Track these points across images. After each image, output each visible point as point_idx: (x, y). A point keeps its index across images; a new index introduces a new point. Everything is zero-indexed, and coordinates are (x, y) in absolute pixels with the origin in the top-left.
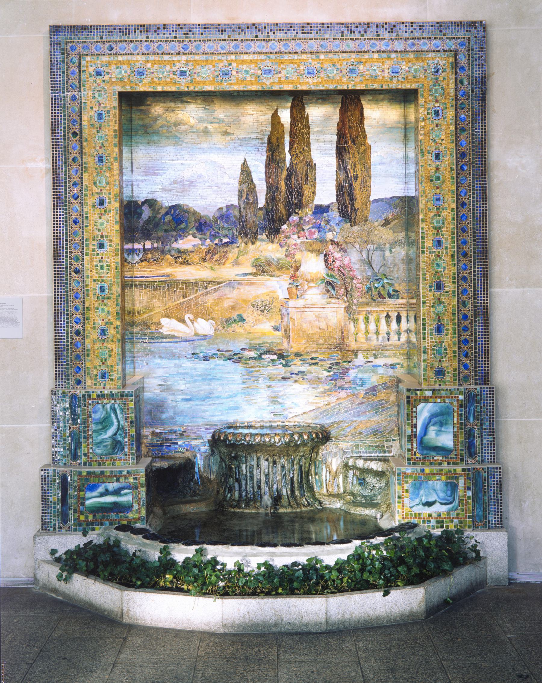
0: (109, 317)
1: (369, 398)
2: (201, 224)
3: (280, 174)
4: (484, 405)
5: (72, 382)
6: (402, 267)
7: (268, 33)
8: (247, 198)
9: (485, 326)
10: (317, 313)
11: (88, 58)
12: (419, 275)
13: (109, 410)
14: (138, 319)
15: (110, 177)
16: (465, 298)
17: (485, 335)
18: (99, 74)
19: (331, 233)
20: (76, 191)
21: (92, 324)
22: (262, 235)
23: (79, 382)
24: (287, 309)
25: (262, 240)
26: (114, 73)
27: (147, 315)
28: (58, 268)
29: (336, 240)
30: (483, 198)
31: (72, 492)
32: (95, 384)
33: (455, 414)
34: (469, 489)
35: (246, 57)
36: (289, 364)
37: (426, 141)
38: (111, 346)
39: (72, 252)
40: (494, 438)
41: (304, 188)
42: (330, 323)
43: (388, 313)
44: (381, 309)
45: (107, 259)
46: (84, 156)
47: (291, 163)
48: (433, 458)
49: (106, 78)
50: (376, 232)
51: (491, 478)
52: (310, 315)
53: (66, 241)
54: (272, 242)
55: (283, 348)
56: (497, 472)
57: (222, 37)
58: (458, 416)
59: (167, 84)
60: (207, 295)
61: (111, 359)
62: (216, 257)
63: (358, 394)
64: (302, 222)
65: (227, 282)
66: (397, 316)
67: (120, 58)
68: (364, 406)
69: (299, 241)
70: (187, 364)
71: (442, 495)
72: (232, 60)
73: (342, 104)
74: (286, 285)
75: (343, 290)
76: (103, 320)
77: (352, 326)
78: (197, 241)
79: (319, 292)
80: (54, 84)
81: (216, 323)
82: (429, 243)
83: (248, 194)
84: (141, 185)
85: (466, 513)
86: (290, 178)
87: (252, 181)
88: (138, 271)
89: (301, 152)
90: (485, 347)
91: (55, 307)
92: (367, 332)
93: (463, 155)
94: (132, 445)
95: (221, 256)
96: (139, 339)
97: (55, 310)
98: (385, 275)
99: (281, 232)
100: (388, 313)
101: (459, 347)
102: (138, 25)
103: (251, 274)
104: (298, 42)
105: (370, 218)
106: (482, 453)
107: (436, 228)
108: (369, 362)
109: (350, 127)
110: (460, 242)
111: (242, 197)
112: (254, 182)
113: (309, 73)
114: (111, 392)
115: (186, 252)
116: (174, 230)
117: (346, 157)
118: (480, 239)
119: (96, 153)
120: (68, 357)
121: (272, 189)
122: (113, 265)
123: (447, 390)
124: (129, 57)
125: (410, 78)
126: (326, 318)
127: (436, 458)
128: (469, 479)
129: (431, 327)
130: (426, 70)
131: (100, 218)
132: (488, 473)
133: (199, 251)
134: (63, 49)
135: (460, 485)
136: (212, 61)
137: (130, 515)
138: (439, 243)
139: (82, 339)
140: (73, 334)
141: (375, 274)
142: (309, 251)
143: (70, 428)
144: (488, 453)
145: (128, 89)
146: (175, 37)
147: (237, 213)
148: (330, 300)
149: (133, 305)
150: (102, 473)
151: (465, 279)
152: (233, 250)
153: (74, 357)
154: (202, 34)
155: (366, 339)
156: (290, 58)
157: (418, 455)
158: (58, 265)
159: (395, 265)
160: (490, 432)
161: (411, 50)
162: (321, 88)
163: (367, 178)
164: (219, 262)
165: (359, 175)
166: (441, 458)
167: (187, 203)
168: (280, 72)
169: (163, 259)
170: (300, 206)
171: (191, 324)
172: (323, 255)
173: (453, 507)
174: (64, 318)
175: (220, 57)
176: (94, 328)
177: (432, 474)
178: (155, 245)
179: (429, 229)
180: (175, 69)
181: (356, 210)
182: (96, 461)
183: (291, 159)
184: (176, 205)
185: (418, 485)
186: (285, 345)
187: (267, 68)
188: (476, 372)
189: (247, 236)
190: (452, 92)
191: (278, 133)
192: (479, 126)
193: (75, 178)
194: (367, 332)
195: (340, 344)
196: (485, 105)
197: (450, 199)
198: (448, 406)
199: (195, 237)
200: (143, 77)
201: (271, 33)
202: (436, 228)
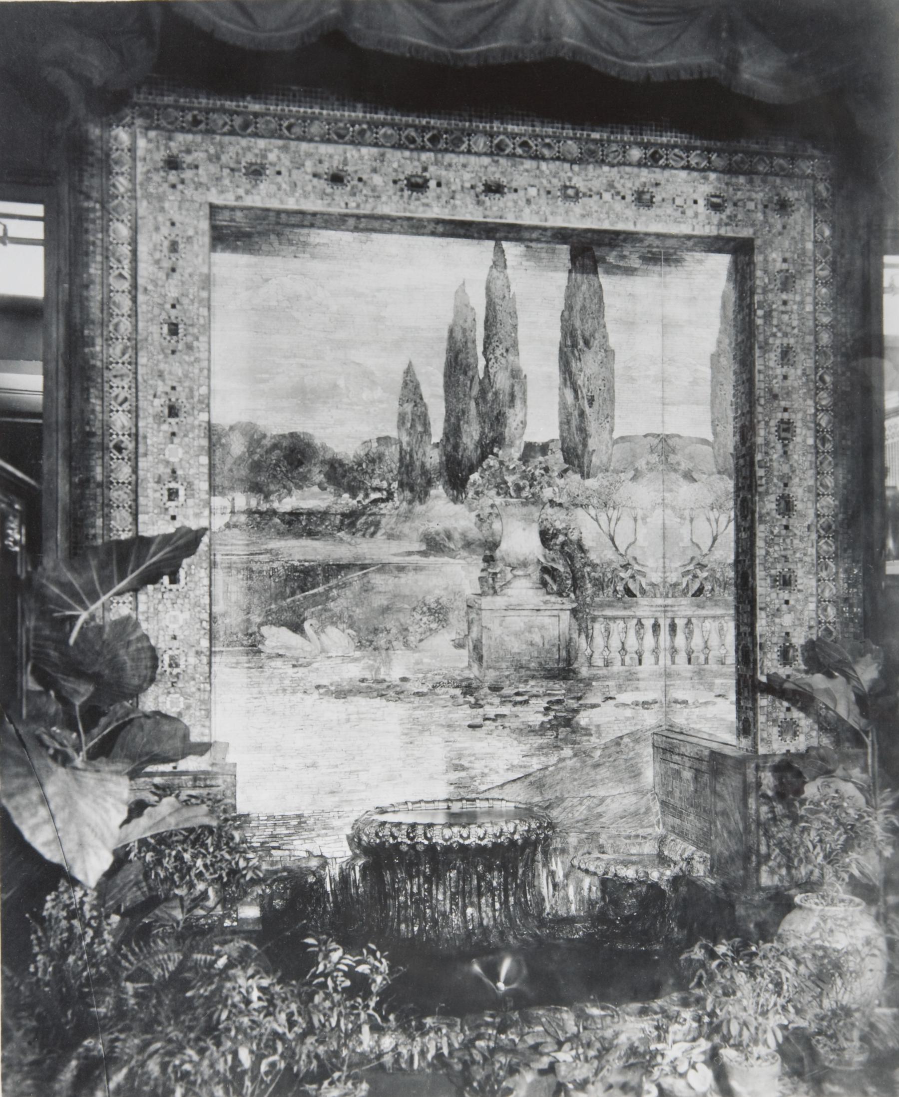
10: (526, 619)
36: (481, 702)
77: (582, 642)
79: (531, 585)
108: (611, 698)
119: (164, 316)
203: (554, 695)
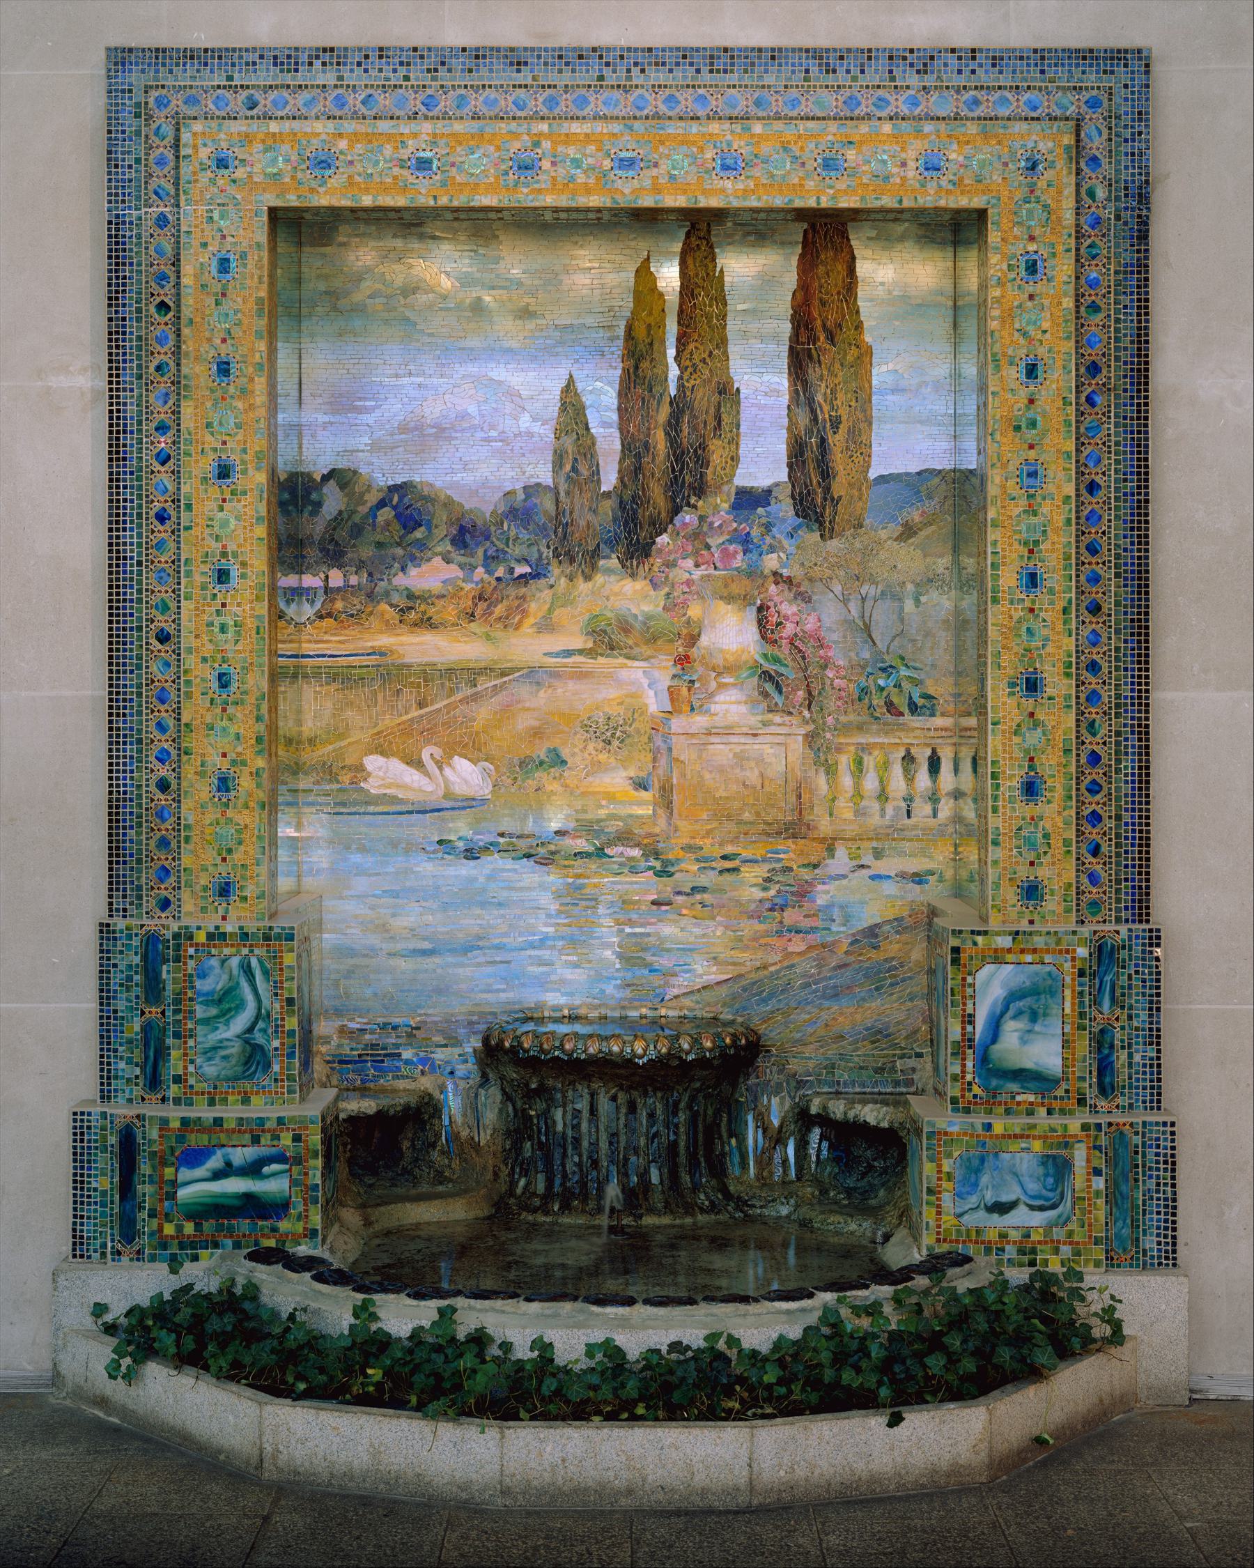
0: (239, 749)
1: (860, 955)
2: (462, 529)
3: (654, 414)
4: (1137, 972)
5: (149, 903)
6: (944, 638)
7: (629, 71)
8: (574, 469)
9: (1140, 782)
10: (738, 749)
11: (198, 127)
12: (985, 656)
13: (235, 972)
14: (309, 756)
15: (246, 411)
16: (1094, 713)
17: (1140, 803)
18: (222, 163)
19: (774, 556)
20: (163, 443)
21: (199, 763)
22: (608, 557)
23: (165, 904)
24: (667, 736)
25: (609, 571)
26: (259, 163)
27: (331, 747)
28: (118, 629)
29: (785, 572)
30: (1139, 473)
31: (145, 1168)
32: (204, 909)
33: (1068, 993)
34: (1097, 1172)
35: (576, 127)
36: (671, 869)
37: (1005, 333)
38: (243, 818)
39: (153, 592)
40: (1159, 1051)
41: (711, 447)
42: (770, 773)
43: (908, 752)
44: (893, 741)
45: (235, 609)
46: (183, 361)
47: (681, 387)
48: (1013, 1098)
49: (240, 173)
50: (883, 555)
51: (1151, 1146)
52: (721, 752)
53: (139, 563)
54: (633, 576)
55: (657, 830)
56: (1164, 1133)
57: (521, 78)
58: (1073, 998)
59: (386, 190)
60: (475, 700)
61: (242, 848)
62: (499, 610)
63: (835, 942)
64: (705, 528)
65: (525, 671)
66: (930, 758)
67: (274, 127)
68: (848, 973)
69: (698, 574)
70: (426, 868)
71: (1033, 1187)
72: (540, 134)
73: (803, 248)
74: (664, 680)
75: (800, 693)
76: (224, 755)
77: (821, 782)
78: (454, 571)
80: (117, 187)
81: (497, 768)
82: (1009, 579)
83: (576, 460)
84: (321, 434)
85: (1090, 1231)
86: (677, 422)
87: (588, 429)
88: (310, 642)
89: (704, 361)
90: (1141, 831)
91: (110, 722)
92: (858, 794)
93: (1094, 369)
94: (291, 1055)
95: (509, 609)
96: (312, 804)
97: (111, 729)
98: (902, 658)
99: (653, 553)
100: (908, 752)
101: (1078, 830)
102: (317, 49)
103: (581, 652)
104: (701, 91)
105: (867, 522)
106: (1130, 1088)
107: (1026, 543)
108: (862, 866)
109: (823, 303)
110: (1083, 578)
111: (561, 466)
112: (592, 431)
113: (725, 167)
114: (241, 928)
115: (426, 598)
116: (399, 544)
117: (813, 373)
118: (1133, 572)
119: (212, 353)
120: (140, 843)
121: (635, 451)
122: (251, 623)
123: (1048, 933)
124: (296, 125)
125: (967, 182)
126: (760, 760)
127: (1019, 1098)
128: (1098, 1148)
129: (1012, 780)
130: (1006, 164)
131: (221, 509)
132: (1143, 1137)
133: (456, 595)
134: (138, 105)
135: (1077, 1163)
136: (494, 135)
137: (284, 1225)
138: (1033, 580)
139: (174, 800)
140: (153, 788)
141: (878, 656)
142: (721, 598)
143: (143, 1013)
144: (1144, 1088)
145: (292, 200)
146: (407, 78)
147: (548, 504)
148: (770, 716)
149: (299, 722)
150: (218, 1122)
151: (1093, 667)
152: (538, 595)
153: (152, 843)
154: (470, 71)
155: (856, 812)
156: (680, 131)
157: (976, 1090)
158: (118, 622)
159: (927, 634)
160: (1151, 1036)
161: (971, 115)
162: (753, 203)
163: (862, 426)
164: (504, 621)
165: (844, 418)
166: (1032, 1098)
167: (431, 480)
168: (656, 165)
169: (371, 613)
170: (700, 489)
171: (437, 771)
172: (755, 609)
173: (1059, 1216)
174: (132, 750)
175: (513, 125)
176: (201, 774)
177: (1009, 1137)
178: (354, 580)
179: (1011, 545)
180: (404, 154)
181: (835, 502)
182: (203, 1093)
183: (680, 378)
184: (405, 483)
185: (976, 1162)
186: (661, 826)
187: (624, 154)
188: (1118, 891)
189: (572, 560)
190: (1069, 217)
191: (650, 314)
192: (1132, 301)
193: (162, 413)
194: (858, 794)
195: (792, 823)
196: (1147, 251)
197: (1061, 475)
198: (1049, 973)
199: (448, 561)
200: (328, 172)
201: (636, 71)
202: (1026, 543)
203: (780, 860)
